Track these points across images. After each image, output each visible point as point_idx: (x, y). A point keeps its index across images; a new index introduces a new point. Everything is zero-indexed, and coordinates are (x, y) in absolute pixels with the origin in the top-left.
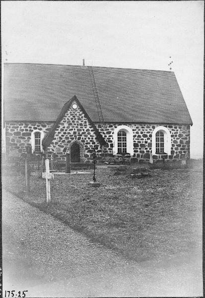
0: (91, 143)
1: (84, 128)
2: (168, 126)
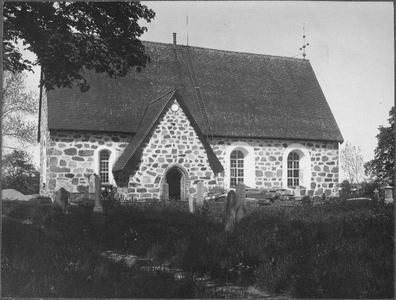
0: (200, 168)
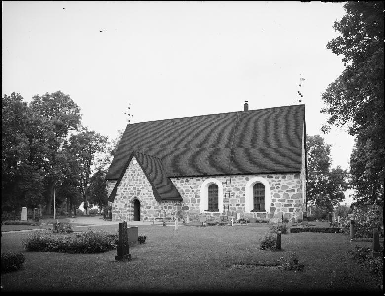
1: (143, 184)
2: (266, 176)
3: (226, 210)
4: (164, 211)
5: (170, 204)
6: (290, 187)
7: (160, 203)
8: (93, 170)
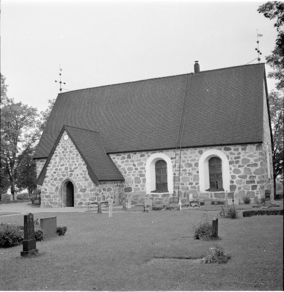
1: (76, 162)
2: (223, 148)
3: (177, 191)
4: (103, 193)
5: (108, 185)
6: (252, 160)
7: (97, 185)
8: (21, 147)
